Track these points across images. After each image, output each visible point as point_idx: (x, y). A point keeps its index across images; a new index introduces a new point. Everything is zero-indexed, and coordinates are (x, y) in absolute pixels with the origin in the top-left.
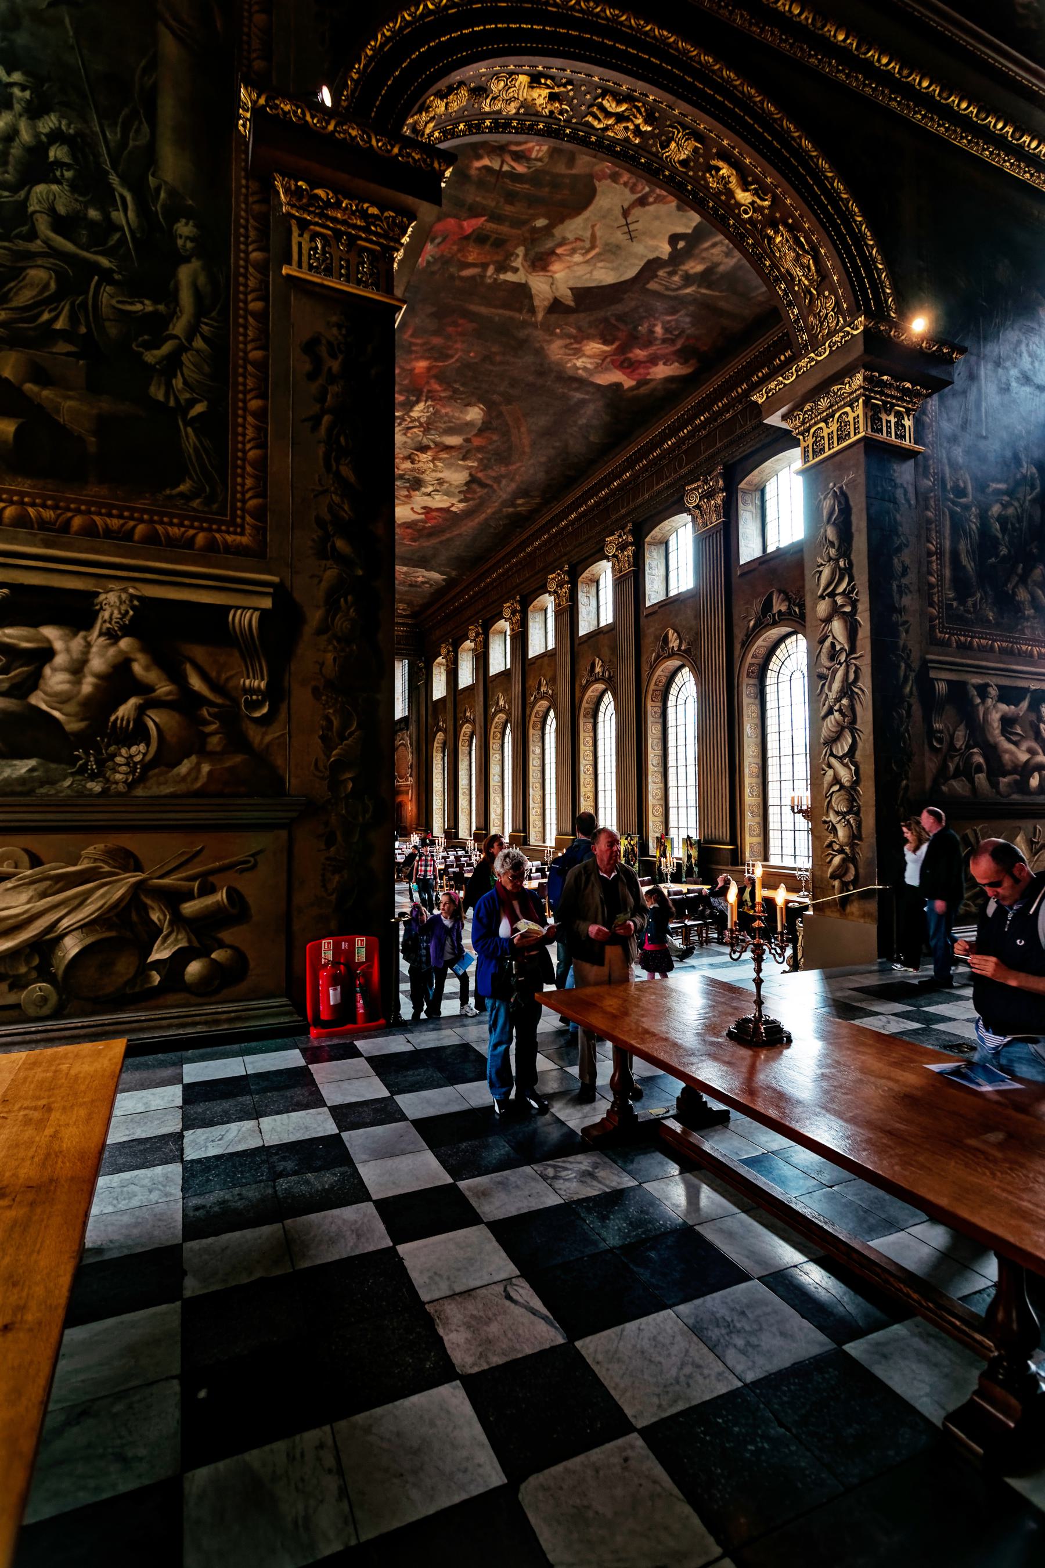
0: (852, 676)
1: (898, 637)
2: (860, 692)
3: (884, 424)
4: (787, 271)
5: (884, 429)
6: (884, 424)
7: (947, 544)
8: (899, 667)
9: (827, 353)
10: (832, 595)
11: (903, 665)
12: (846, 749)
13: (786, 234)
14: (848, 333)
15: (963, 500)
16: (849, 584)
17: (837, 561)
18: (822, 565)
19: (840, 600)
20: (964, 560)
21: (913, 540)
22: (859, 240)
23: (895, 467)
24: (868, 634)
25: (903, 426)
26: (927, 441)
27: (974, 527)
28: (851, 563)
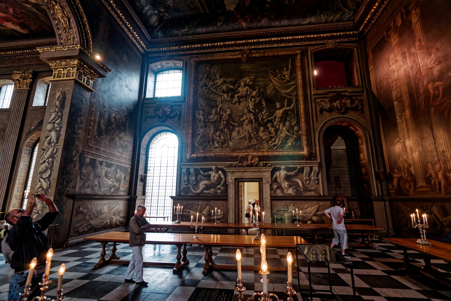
0: (55, 151)
1: (75, 142)
2: (56, 157)
3: (83, 78)
4: (59, 18)
5: (83, 80)
6: (83, 78)
7: (97, 119)
8: (73, 151)
9: (67, 49)
10: (54, 123)
11: (75, 151)
12: (47, 176)
13: (59, 7)
14: (74, 47)
15: (104, 109)
16: (60, 121)
17: (58, 113)
18: (52, 112)
19: (56, 125)
20: (102, 125)
21: (86, 114)
22: (84, 25)
23: (84, 92)
24: (64, 139)
25: (89, 82)
26: (96, 89)
27: (106, 117)
28: (62, 115)
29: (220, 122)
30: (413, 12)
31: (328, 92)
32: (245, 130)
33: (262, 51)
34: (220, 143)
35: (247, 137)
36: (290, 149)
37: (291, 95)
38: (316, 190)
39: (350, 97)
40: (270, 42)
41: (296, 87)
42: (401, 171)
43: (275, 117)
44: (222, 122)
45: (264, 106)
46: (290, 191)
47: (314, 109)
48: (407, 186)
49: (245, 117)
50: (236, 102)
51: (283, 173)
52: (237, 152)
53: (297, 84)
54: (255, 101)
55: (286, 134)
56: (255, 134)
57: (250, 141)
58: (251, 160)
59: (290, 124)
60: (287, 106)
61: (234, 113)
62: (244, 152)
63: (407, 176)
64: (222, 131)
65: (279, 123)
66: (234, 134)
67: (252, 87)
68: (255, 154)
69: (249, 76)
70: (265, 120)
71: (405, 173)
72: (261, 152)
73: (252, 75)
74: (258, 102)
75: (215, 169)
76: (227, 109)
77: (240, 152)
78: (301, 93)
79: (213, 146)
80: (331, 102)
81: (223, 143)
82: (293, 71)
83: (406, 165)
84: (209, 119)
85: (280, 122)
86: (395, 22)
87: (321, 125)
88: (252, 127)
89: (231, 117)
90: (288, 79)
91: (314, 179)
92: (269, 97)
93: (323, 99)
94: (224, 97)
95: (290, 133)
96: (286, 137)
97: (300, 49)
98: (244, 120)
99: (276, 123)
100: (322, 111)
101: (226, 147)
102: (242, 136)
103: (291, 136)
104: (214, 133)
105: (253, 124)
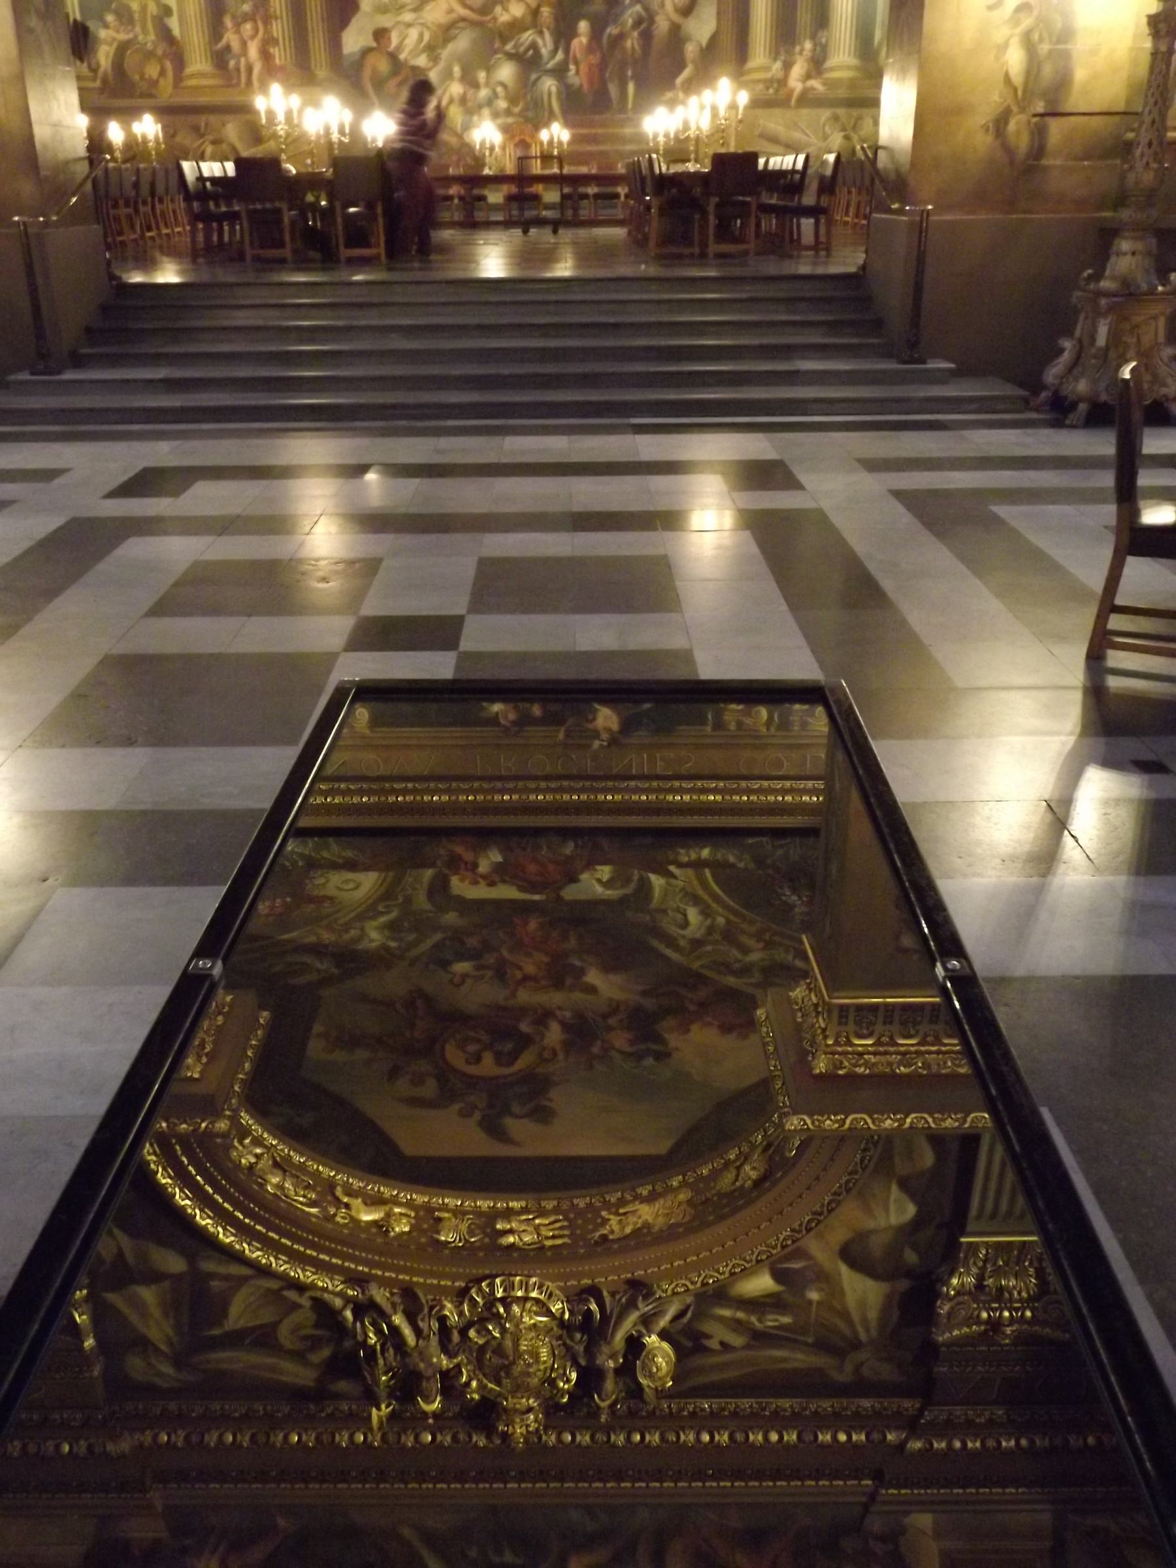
48: (152, 71)
63: (153, 42)
71: (145, 31)
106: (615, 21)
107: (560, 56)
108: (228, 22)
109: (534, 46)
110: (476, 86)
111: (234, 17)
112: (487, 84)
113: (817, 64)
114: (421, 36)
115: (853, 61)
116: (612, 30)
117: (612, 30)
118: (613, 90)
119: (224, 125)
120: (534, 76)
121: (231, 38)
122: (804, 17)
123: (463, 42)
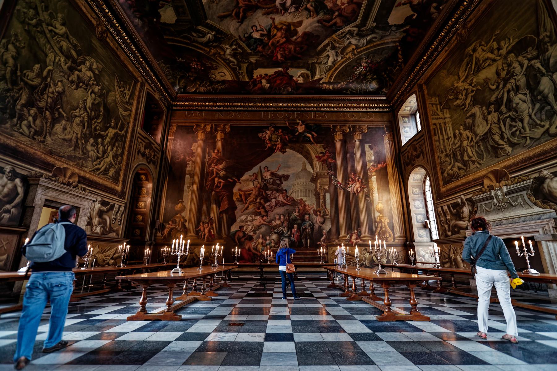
29: (42, 94)
30: (219, 132)
31: (146, 138)
32: (74, 132)
33: (117, 45)
34: (33, 130)
35: (73, 142)
36: (109, 179)
37: (125, 119)
38: (117, 232)
39: (154, 151)
40: (127, 45)
41: (130, 114)
42: (176, 223)
43: (107, 135)
44: (45, 96)
45: (101, 113)
46: (98, 230)
47: (135, 147)
49: (77, 113)
50: (72, 82)
51: (98, 205)
52: (54, 158)
53: (130, 111)
54: (95, 100)
55: (111, 161)
56: (82, 144)
57: (75, 150)
58: (70, 177)
59: (117, 151)
60: (120, 131)
61: (66, 96)
62: (63, 162)
64: (40, 110)
65: (108, 145)
66: (58, 128)
67: (98, 78)
68: (77, 171)
69: (97, 62)
70: (98, 132)
71: (178, 226)
72: (84, 171)
73: (100, 64)
74: (98, 103)
75: (9, 172)
76: (58, 81)
77: (59, 160)
78: (131, 124)
79: (18, 129)
80: (146, 148)
81: (36, 133)
82: (132, 96)
83: (182, 220)
84: (25, 74)
85: (109, 142)
86: (205, 126)
87: (136, 166)
88: (82, 132)
89: (61, 98)
90: (127, 101)
91: (119, 219)
92: (108, 107)
93: (142, 142)
94: (60, 60)
95: (114, 161)
96: (110, 163)
97: (142, 79)
98: (76, 116)
99: (106, 142)
100: (139, 152)
101: (41, 142)
102: (67, 137)
103: (114, 166)
104: (23, 106)
105: (84, 129)
106: (304, 225)
107: (289, 233)
108: (201, 224)
109: (282, 230)
110: (266, 240)
111: (203, 223)
112: (269, 240)
113: (359, 236)
114: (252, 227)
115: (369, 235)
116: (303, 227)
117: (303, 227)
118: (303, 241)
119: (195, 249)
120: (282, 238)
121: (201, 228)
122: (354, 225)
123: (263, 229)
